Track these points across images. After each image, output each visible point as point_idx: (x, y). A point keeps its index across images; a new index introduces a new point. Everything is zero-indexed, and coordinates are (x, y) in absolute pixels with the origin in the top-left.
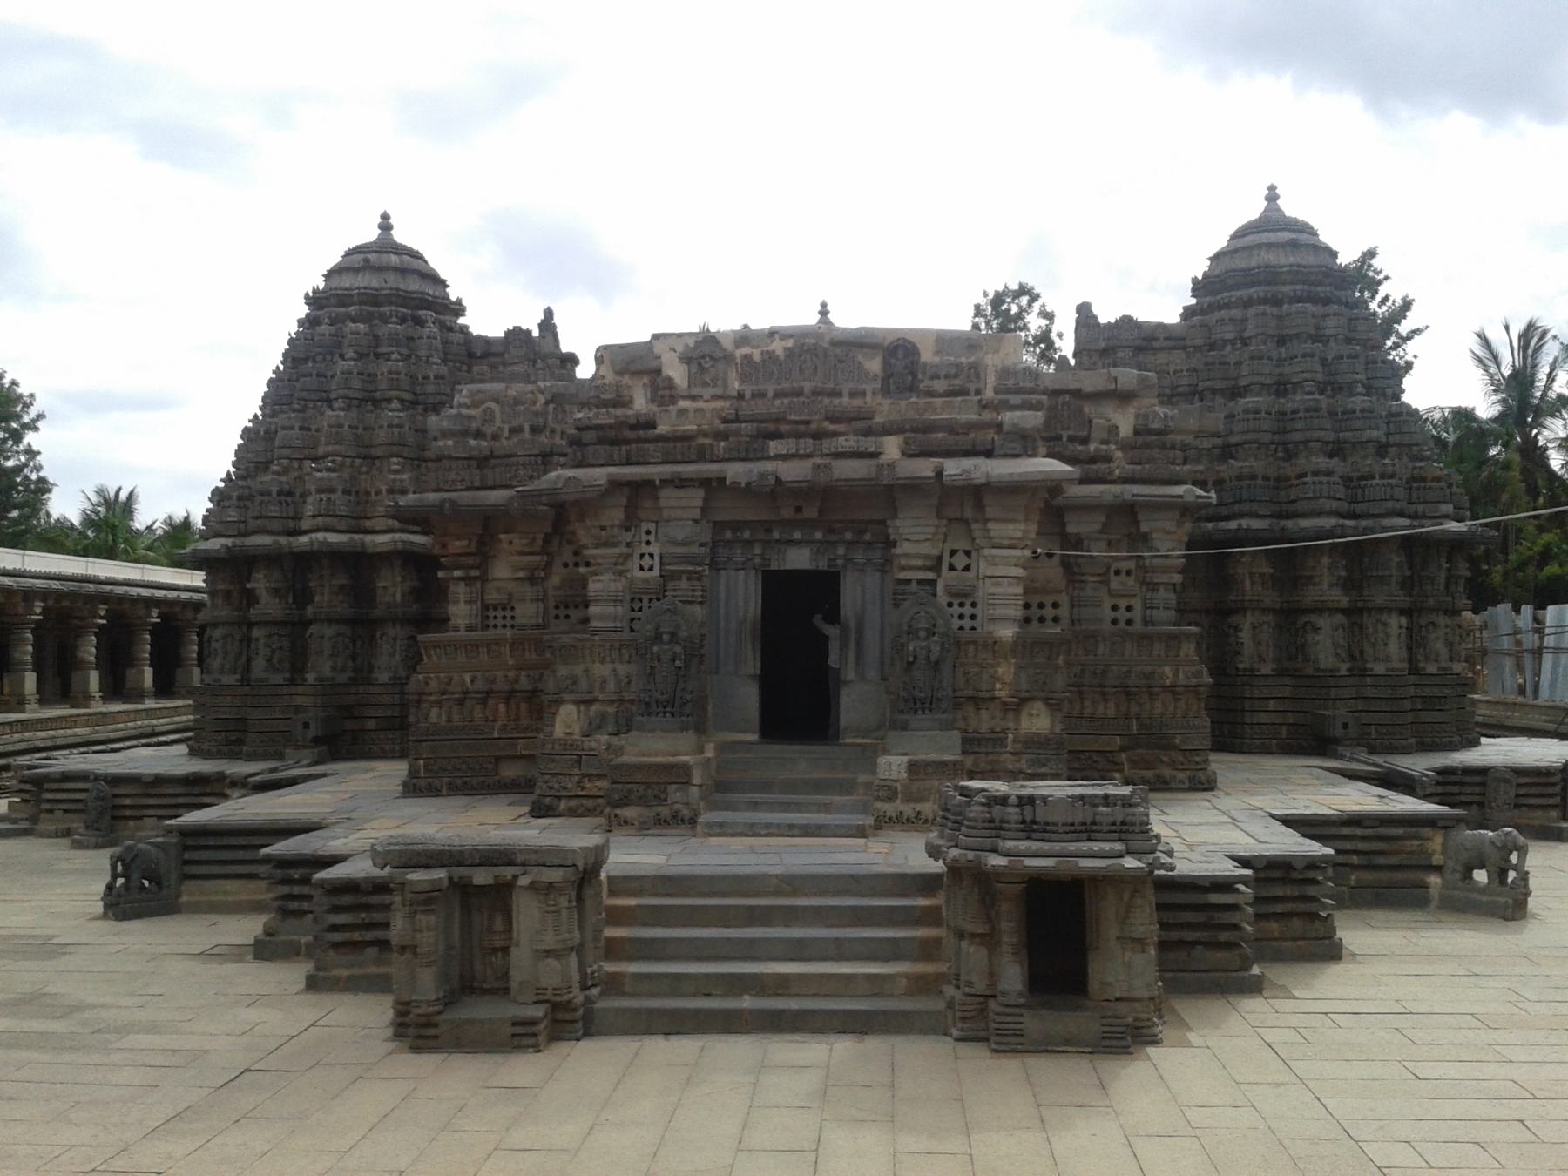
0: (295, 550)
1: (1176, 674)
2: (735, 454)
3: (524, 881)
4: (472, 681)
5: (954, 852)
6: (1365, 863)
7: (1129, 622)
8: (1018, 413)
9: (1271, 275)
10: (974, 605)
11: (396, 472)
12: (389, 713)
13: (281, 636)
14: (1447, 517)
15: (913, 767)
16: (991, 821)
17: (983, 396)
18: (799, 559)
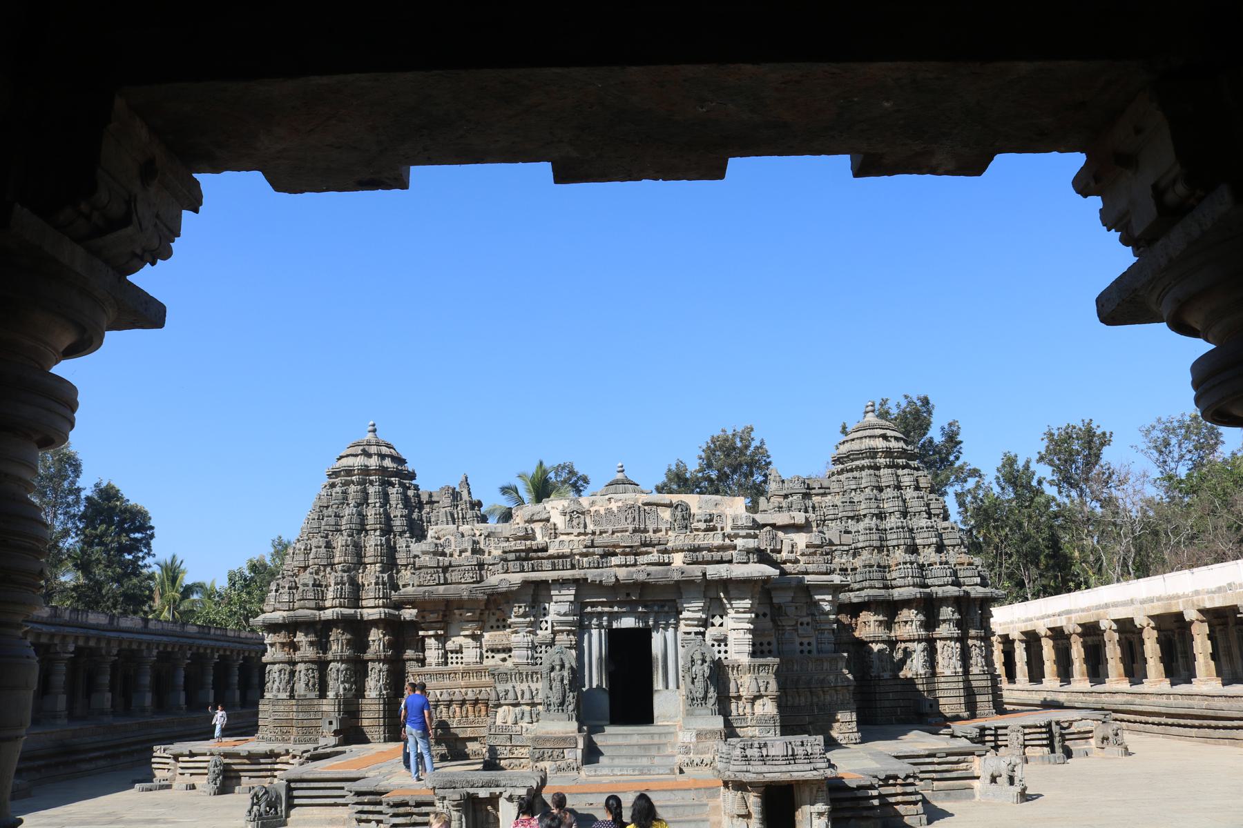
0: (323, 619)
1: (836, 679)
2: (592, 565)
3: (506, 795)
4: (441, 695)
5: (727, 773)
6: (939, 777)
7: (810, 652)
8: (745, 540)
9: (873, 453)
10: (726, 645)
11: (382, 572)
12: (377, 716)
13: (313, 670)
14: (977, 585)
15: (699, 735)
16: (746, 756)
17: (725, 531)
18: (628, 622)
